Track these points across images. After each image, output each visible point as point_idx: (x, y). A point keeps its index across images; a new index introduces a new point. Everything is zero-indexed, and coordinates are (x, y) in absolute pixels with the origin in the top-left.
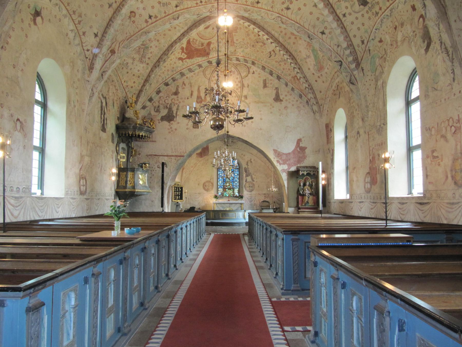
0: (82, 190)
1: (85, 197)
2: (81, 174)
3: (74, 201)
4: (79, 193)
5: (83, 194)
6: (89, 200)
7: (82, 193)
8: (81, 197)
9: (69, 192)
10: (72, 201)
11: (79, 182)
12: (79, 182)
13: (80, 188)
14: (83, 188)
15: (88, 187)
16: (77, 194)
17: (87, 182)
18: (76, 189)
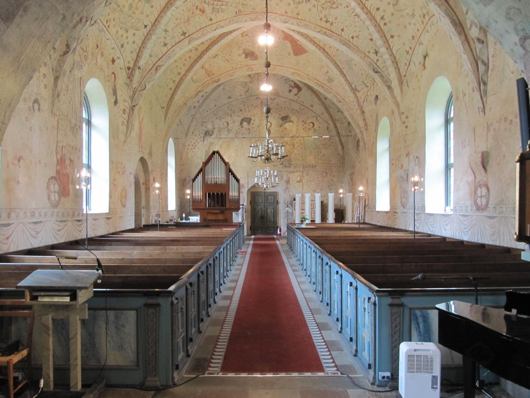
0: (479, 204)
1: (485, 213)
2: (477, 181)
3: (465, 219)
4: (474, 208)
5: (482, 209)
6: (495, 220)
7: (479, 208)
8: (479, 213)
9: (458, 208)
10: (462, 218)
11: (475, 193)
12: (475, 193)
13: (475, 201)
14: (482, 202)
15: (491, 199)
16: (471, 210)
17: (491, 190)
18: (469, 203)
